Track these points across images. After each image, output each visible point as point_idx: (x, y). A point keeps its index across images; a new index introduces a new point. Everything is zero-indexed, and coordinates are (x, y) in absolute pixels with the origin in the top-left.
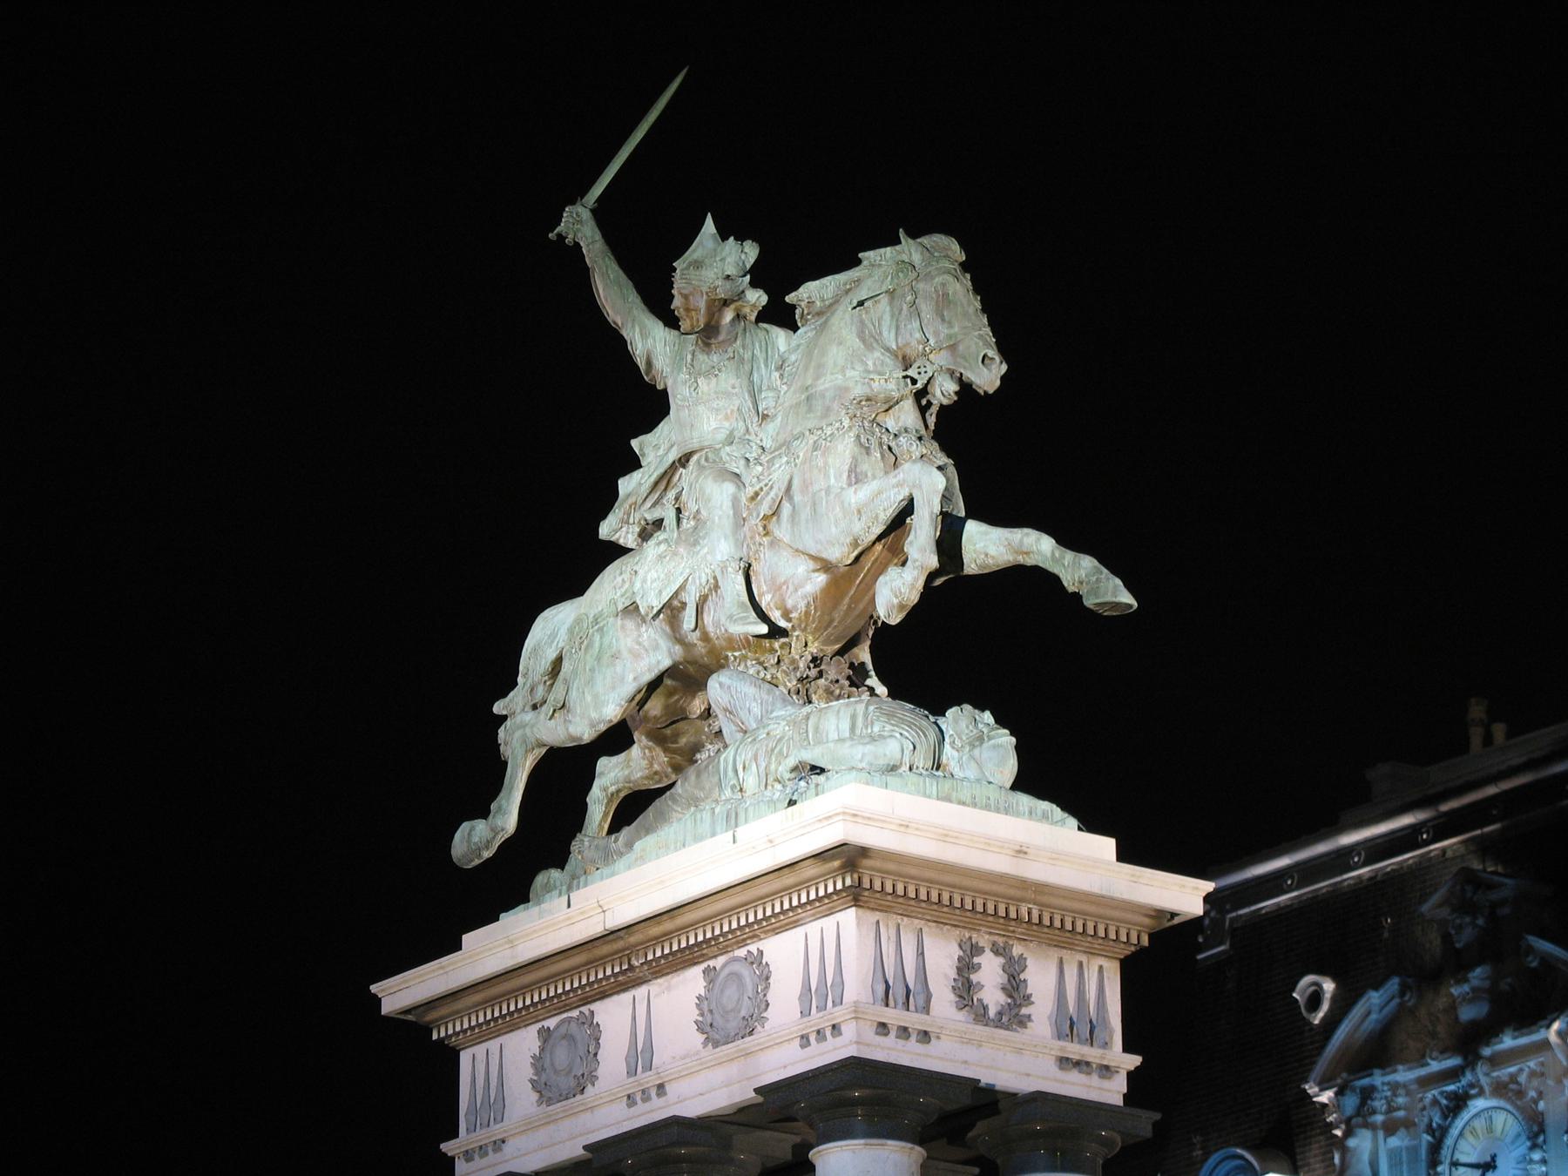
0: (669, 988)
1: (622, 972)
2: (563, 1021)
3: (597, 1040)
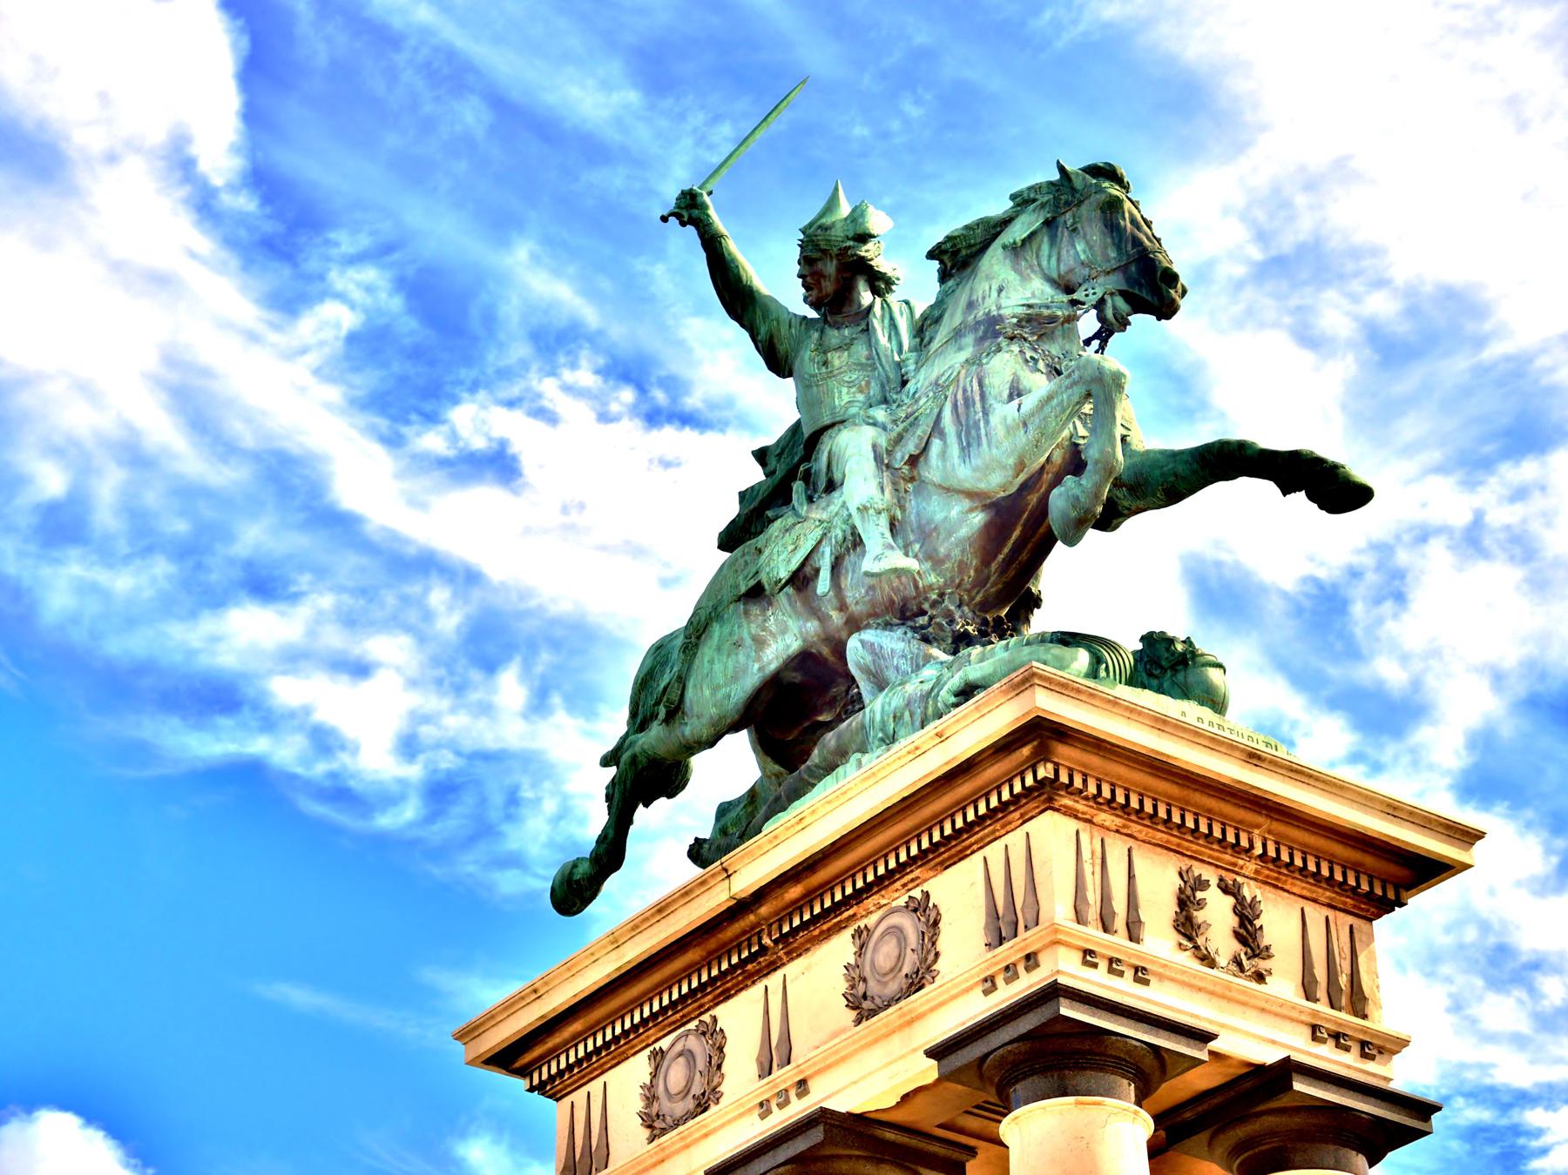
1: (753, 957)
3: (721, 1049)
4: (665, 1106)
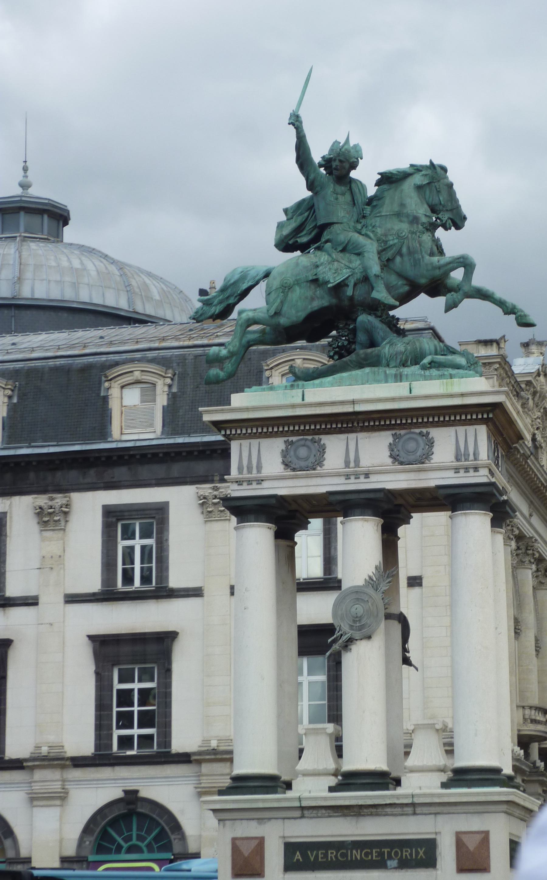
0: (369, 437)
2: (301, 440)
4: (295, 460)
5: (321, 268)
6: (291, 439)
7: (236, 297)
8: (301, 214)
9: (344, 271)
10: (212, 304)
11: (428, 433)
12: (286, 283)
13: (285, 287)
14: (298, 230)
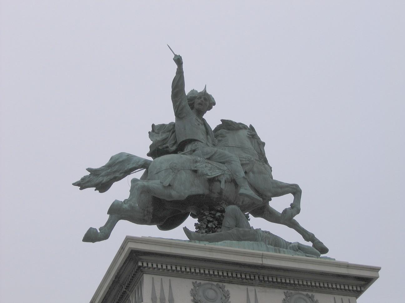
2: (207, 284)
5: (198, 164)
6: (198, 281)
7: (121, 173)
8: (164, 132)
9: (217, 170)
10: (99, 175)
11: (313, 296)
12: (176, 166)
13: (175, 169)
14: (164, 140)
